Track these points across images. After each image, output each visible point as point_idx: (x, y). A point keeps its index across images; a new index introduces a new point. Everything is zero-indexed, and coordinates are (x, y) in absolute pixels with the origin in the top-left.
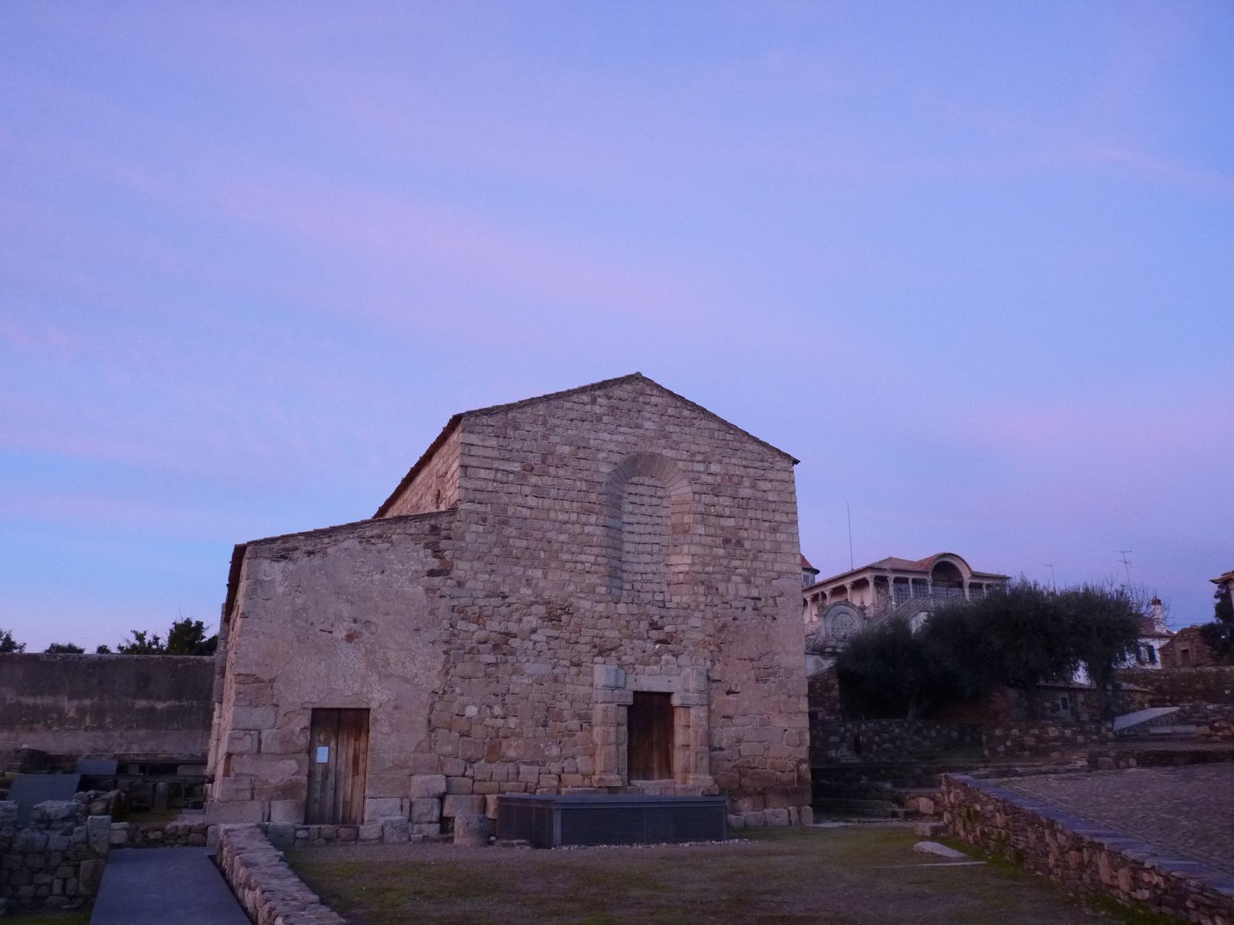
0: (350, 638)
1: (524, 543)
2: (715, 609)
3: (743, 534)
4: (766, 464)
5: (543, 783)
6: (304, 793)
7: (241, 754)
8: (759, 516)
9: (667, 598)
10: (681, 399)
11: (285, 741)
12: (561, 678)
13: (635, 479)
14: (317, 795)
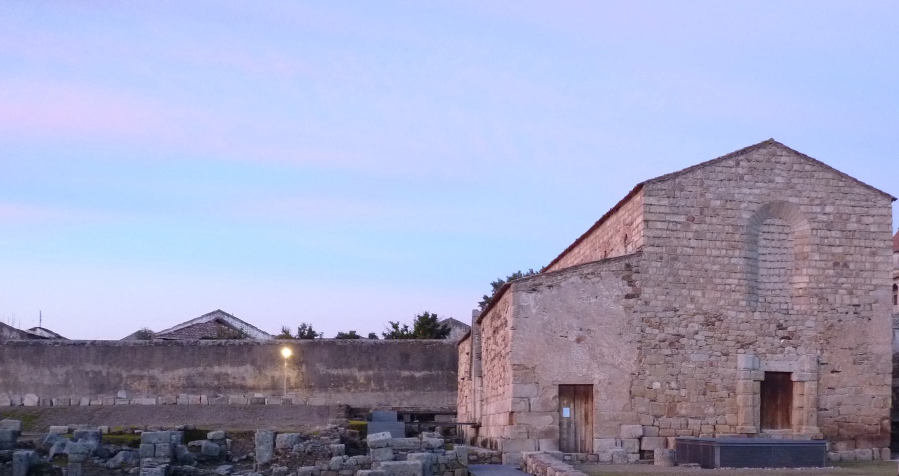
0: (579, 340)
1: (689, 273)
2: (825, 314)
3: (849, 258)
4: (870, 203)
5: (703, 430)
6: (558, 435)
7: (519, 412)
8: (863, 244)
9: (790, 307)
10: (805, 156)
11: (544, 404)
12: (715, 364)
13: (768, 221)
14: (565, 436)
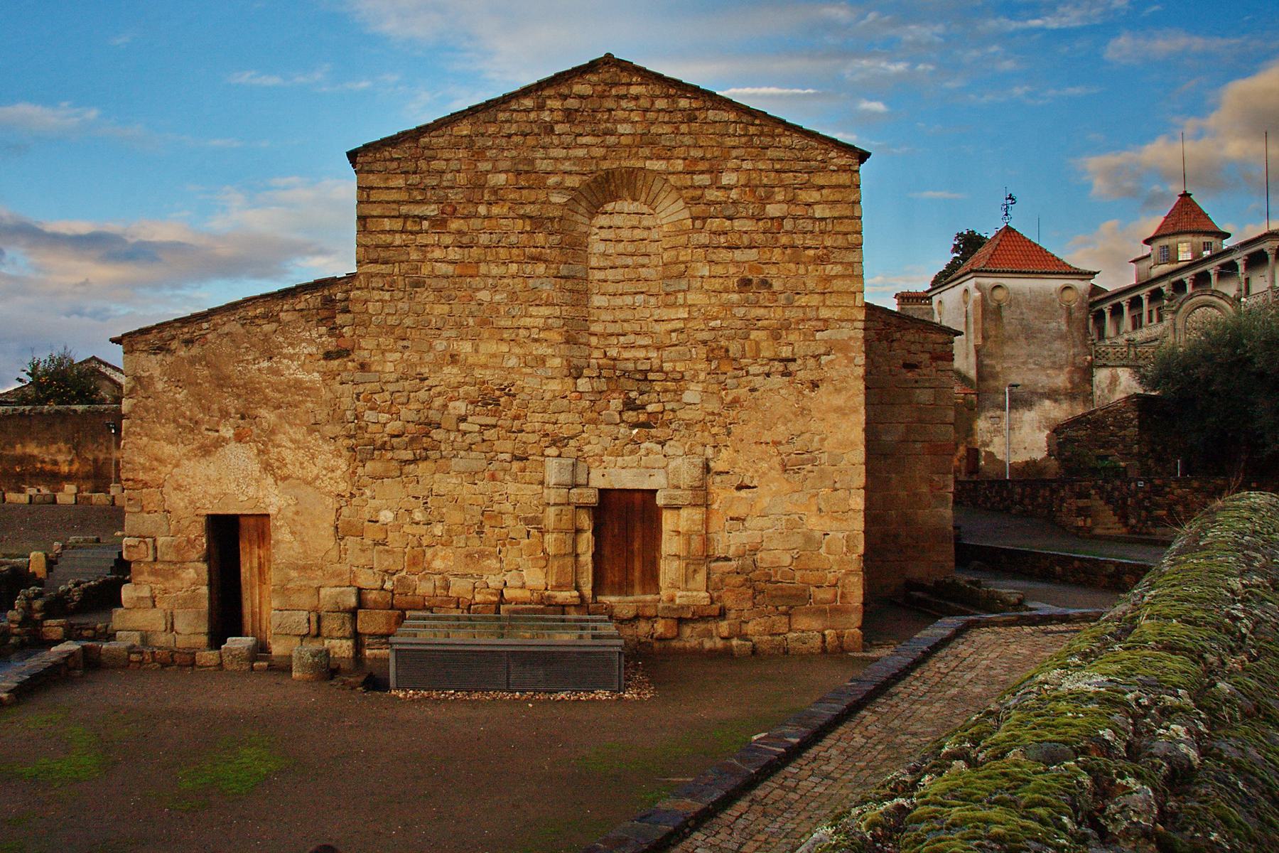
13: (609, 207)
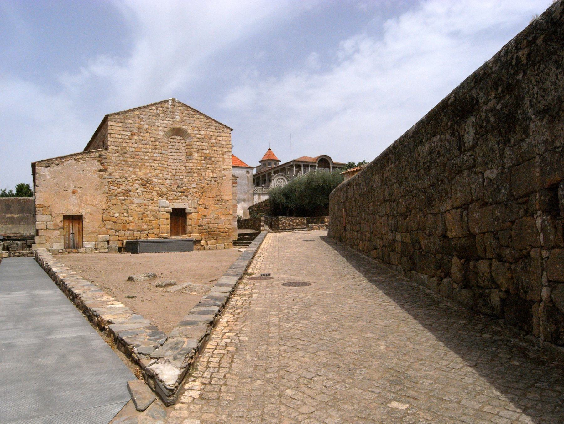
0: (73, 192)
1: (132, 160)
3: (212, 155)
11: (56, 225)
12: (147, 204)
